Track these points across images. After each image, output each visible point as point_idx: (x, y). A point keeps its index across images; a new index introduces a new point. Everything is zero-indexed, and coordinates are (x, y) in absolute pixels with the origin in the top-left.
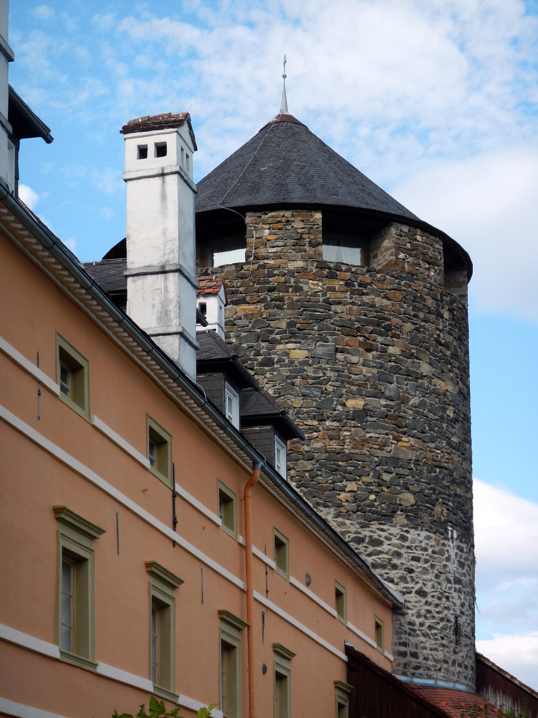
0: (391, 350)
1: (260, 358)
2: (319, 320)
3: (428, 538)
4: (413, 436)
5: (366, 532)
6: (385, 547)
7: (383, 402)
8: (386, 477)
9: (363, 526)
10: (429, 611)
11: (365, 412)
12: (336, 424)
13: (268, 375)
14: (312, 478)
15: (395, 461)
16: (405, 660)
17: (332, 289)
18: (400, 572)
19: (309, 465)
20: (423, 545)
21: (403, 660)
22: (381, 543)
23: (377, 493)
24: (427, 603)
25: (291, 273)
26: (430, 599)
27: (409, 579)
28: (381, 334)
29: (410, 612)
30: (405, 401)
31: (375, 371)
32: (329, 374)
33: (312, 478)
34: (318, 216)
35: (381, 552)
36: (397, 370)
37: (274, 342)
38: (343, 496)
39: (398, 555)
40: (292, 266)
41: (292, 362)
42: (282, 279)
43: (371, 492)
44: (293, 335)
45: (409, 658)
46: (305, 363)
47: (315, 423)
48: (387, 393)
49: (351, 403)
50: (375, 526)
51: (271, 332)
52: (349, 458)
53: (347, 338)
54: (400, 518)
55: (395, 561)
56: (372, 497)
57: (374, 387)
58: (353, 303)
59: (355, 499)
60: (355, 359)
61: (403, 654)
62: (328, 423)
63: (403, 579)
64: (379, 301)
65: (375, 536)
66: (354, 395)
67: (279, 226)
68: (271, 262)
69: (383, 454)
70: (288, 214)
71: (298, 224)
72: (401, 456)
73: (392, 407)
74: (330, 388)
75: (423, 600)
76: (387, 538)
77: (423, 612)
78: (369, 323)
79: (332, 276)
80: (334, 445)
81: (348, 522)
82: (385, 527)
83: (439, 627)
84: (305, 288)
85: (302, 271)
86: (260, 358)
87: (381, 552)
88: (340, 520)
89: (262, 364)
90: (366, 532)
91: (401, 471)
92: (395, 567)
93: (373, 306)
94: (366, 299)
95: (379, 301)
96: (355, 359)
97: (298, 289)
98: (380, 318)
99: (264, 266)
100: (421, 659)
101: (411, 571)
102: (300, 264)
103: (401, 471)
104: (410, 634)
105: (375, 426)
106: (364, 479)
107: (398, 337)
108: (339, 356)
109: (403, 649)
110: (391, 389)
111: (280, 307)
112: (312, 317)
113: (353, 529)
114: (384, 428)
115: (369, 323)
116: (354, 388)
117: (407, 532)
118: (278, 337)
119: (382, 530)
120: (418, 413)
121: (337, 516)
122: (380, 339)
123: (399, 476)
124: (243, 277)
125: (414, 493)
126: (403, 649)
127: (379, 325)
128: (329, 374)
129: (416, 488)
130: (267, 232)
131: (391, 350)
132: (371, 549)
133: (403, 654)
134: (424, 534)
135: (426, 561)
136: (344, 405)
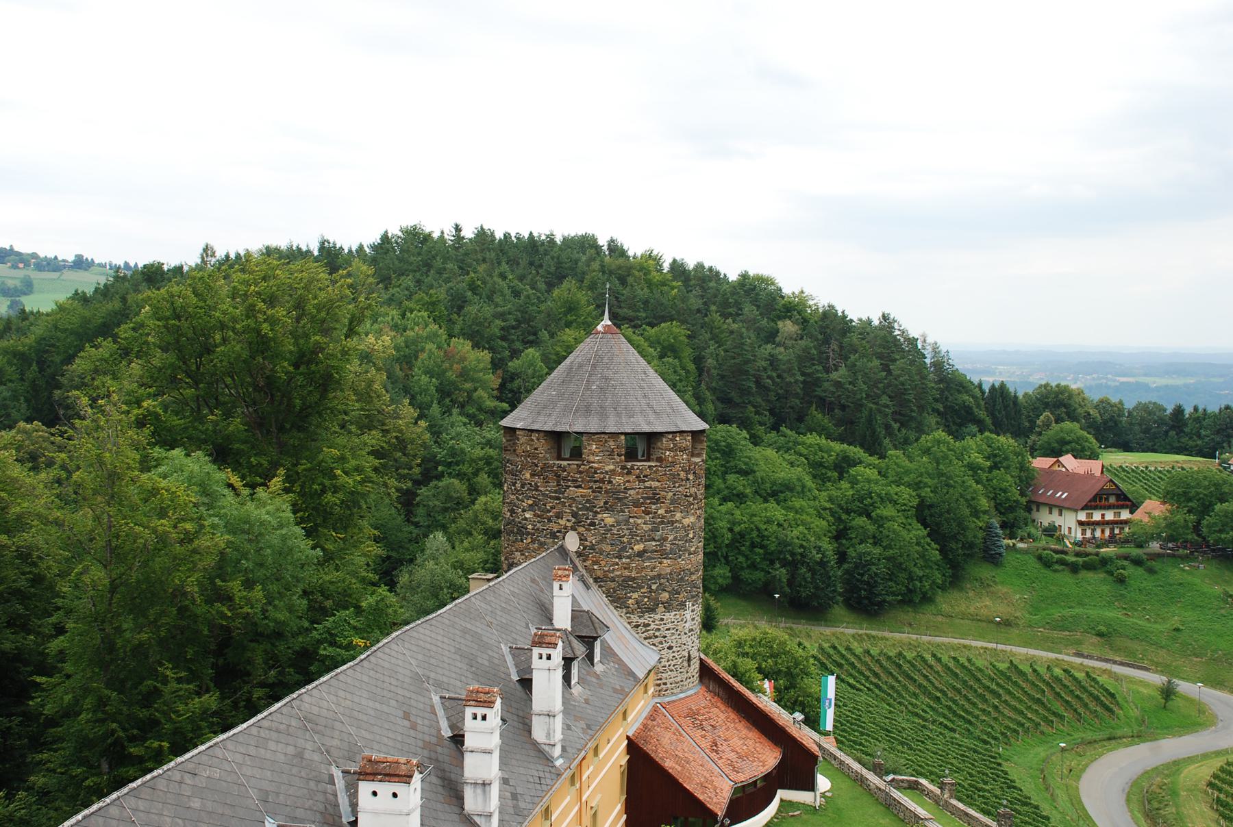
0: (660, 512)
1: (589, 521)
2: (620, 499)
4: (670, 558)
5: (642, 621)
7: (654, 543)
9: (640, 617)
11: (645, 551)
12: (628, 560)
13: (593, 532)
14: (615, 592)
17: (628, 481)
19: (613, 585)
22: (649, 625)
23: (648, 598)
25: (607, 473)
28: (654, 504)
30: (665, 539)
31: (650, 526)
32: (625, 531)
33: (615, 592)
34: (623, 437)
36: (662, 522)
37: (596, 513)
38: (630, 601)
40: (608, 468)
41: (605, 525)
42: (602, 476)
43: (646, 597)
44: (607, 509)
46: (613, 526)
47: (617, 560)
48: (657, 538)
50: (647, 615)
51: (595, 507)
52: (633, 579)
53: (636, 509)
54: (661, 609)
56: (646, 600)
57: (649, 536)
58: (640, 488)
62: (624, 560)
65: (646, 622)
66: (638, 542)
67: (601, 443)
68: (596, 465)
69: (652, 574)
70: (606, 437)
71: (612, 443)
74: (625, 540)
78: (648, 498)
79: (629, 473)
80: (626, 573)
81: (632, 616)
82: (652, 616)
84: (614, 482)
85: (613, 471)
86: (589, 521)
88: (628, 615)
89: (590, 525)
90: (642, 621)
93: (651, 488)
94: (647, 484)
96: (639, 521)
97: (610, 482)
98: (653, 494)
99: (592, 467)
102: (612, 467)
105: (650, 558)
106: (642, 590)
108: (631, 520)
111: (600, 492)
112: (617, 498)
113: (635, 620)
114: (655, 558)
115: (648, 498)
116: (638, 538)
118: (599, 510)
120: (673, 544)
121: (626, 613)
122: (654, 507)
124: (581, 472)
128: (625, 531)
130: (594, 446)
131: (660, 512)
132: (644, 629)
136: (633, 549)
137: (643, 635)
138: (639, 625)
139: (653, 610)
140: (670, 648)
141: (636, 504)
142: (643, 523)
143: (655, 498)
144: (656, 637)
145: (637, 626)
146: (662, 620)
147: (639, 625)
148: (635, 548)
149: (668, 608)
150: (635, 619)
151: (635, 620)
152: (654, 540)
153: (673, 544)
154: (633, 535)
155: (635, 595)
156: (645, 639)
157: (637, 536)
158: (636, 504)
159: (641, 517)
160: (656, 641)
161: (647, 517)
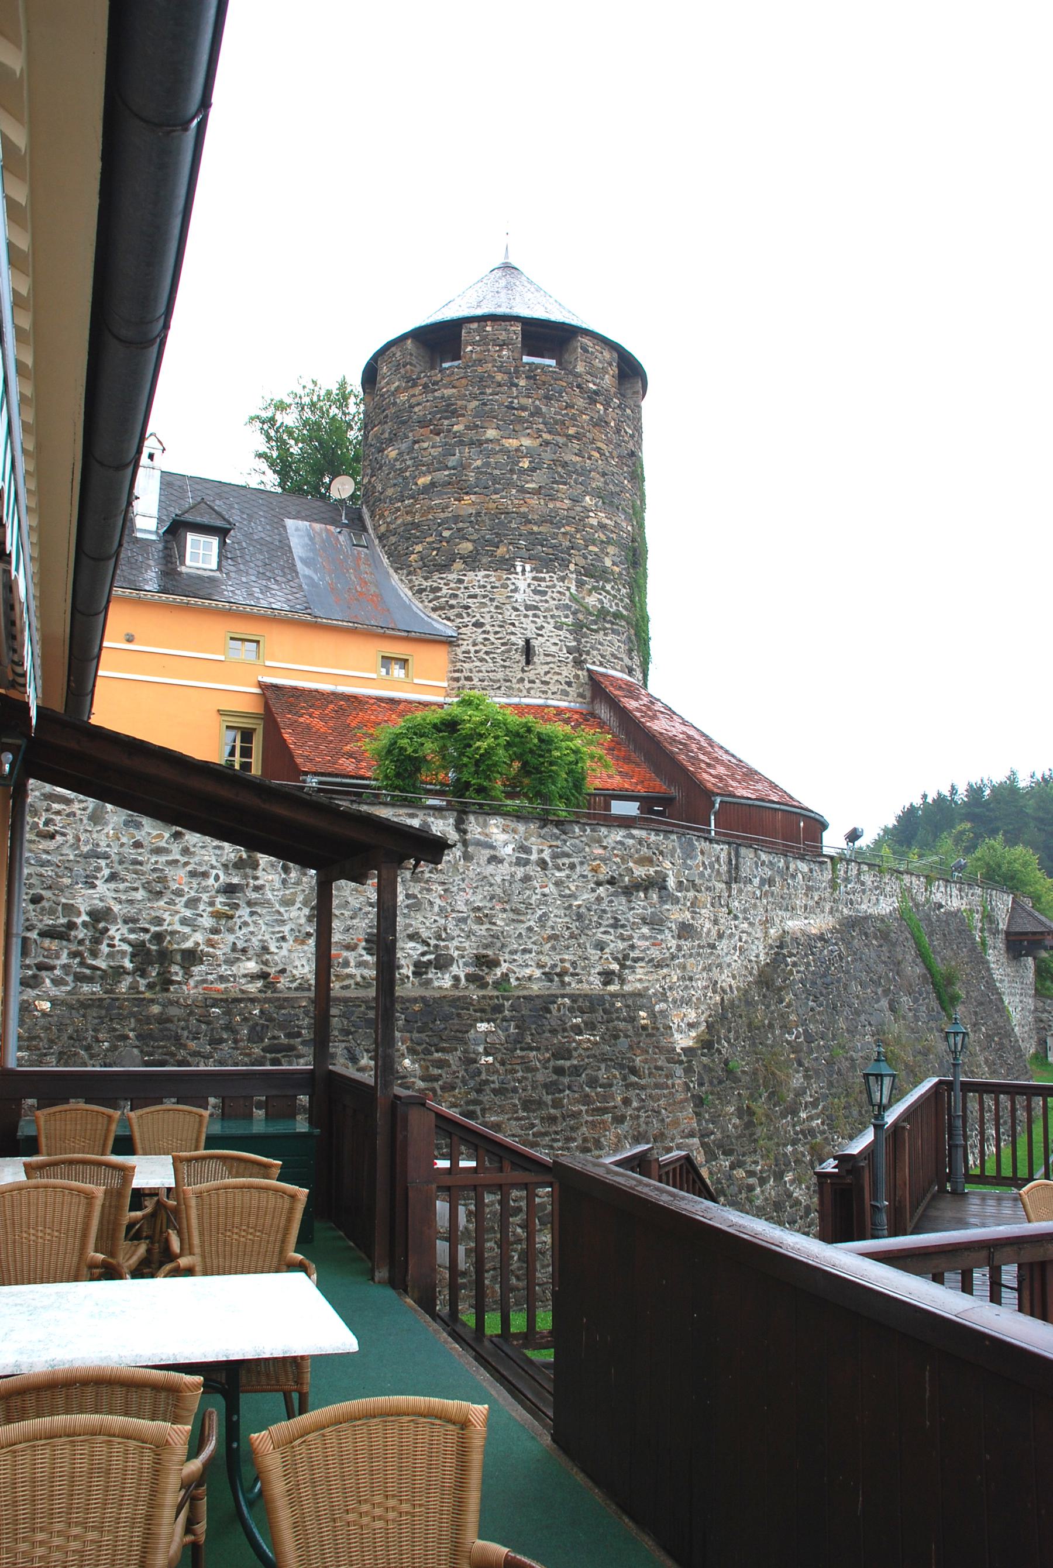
3: (487, 576)
6: (444, 591)
8: (446, 534)
10: (486, 639)
11: (433, 484)
15: (457, 518)
16: (459, 684)
18: (456, 611)
20: (482, 583)
21: (456, 685)
24: (484, 632)
26: (488, 628)
27: (465, 615)
29: (465, 643)
31: (440, 449)
35: (439, 597)
39: (455, 596)
43: (434, 549)
45: (463, 682)
48: (450, 464)
49: (421, 481)
50: (436, 576)
52: (416, 526)
54: (458, 565)
55: (452, 602)
56: (435, 553)
59: (422, 559)
60: (425, 445)
61: (457, 680)
63: (460, 616)
64: (448, 392)
65: (435, 584)
72: (462, 513)
73: (454, 475)
75: (480, 630)
76: (445, 584)
77: (480, 639)
82: (444, 576)
83: (499, 651)
87: (439, 597)
91: (461, 525)
92: (452, 607)
95: (448, 392)
100: (476, 682)
101: (467, 607)
103: (461, 525)
104: (464, 662)
105: (440, 494)
107: (463, 415)
109: (457, 675)
110: (452, 461)
114: (449, 493)
117: (465, 575)
119: (442, 578)
123: (459, 530)
125: (474, 541)
126: (457, 675)
127: (446, 411)
129: (475, 537)
132: (431, 596)
133: (457, 680)
134: (483, 573)
135: (484, 597)
137: (431, 605)
138: (425, 590)
139: (445, 568)
140: (478, 625)
141: (423, 423)
142: (431, 447)
143: (451, 411)
144: (452, 607)
145: (421, 591)
146: (461, 581)
147: (425, 590)
148: (419, 482)
149: (472, 562)
150: (418, 581)
151: (417, 583)
152: (447, 468)
153: (481, 473)
154: (417, 465)
155: (419, 548)
156: (434, 609)
157: (424, 465)
158: (423, 423)
159: (429, 439)
160: (451, 613)
161: (438, 439)
